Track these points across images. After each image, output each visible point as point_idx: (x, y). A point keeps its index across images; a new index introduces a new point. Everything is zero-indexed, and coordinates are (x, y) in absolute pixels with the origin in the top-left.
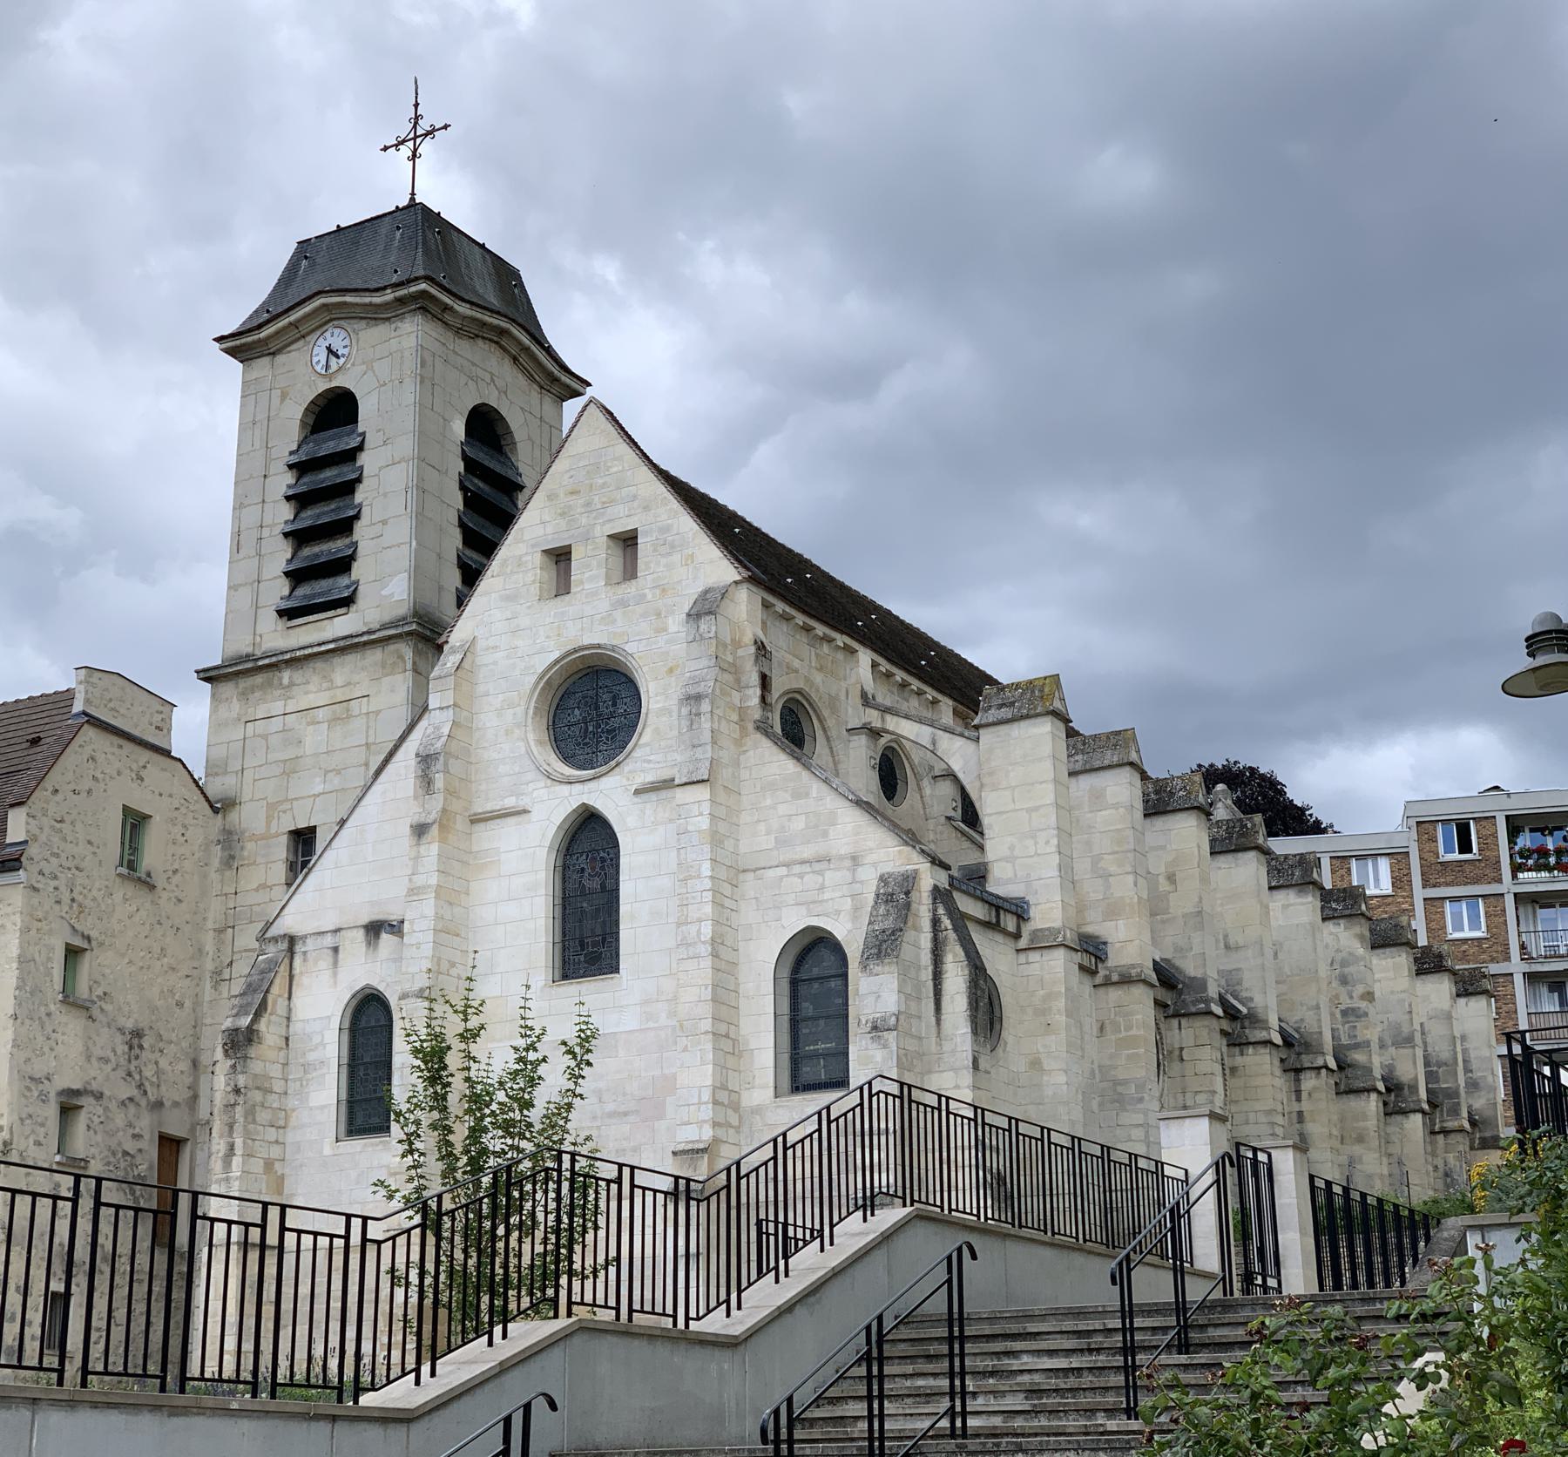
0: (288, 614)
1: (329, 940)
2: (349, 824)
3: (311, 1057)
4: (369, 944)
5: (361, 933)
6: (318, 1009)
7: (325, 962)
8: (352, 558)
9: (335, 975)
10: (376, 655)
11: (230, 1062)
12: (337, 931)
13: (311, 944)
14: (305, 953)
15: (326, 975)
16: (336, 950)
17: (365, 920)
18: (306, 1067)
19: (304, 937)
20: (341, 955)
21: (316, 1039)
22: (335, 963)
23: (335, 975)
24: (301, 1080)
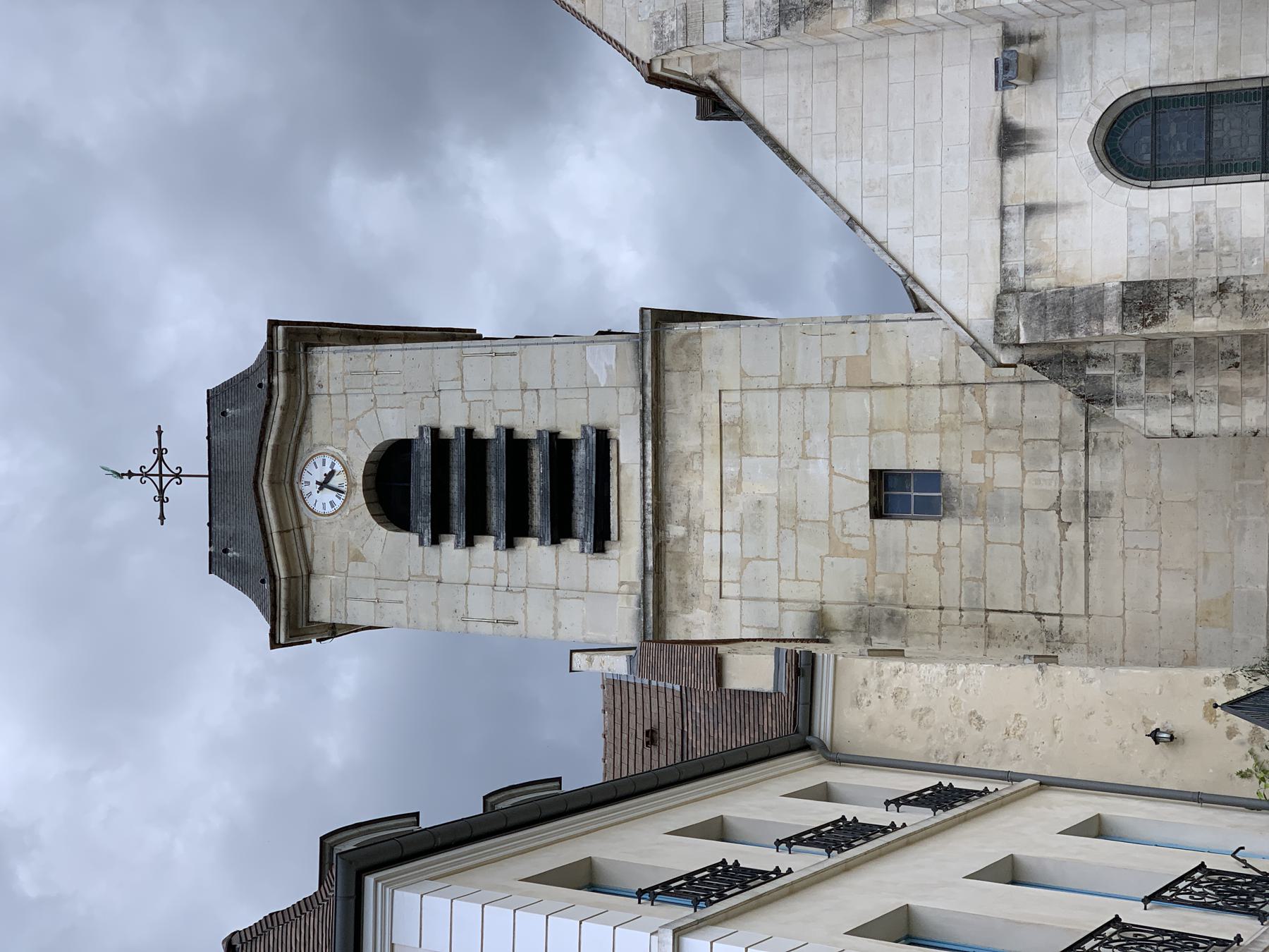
0: (601, 539)
1: (1014, 226)
2: (857, 214)
3: (1186, 239)
4: (1030, 148)
5: (1015, 166)
6: (1112, 232)
7: (1045, 227)
8: (554, 435)
9: (1067, 207)
10: (673, 380)
11: (1175, 311)
12: (1003, 214)
13: (1016, 261)
14: (1027, 270)
15: (1066, 223)
16: (1030, 210)
17: (994, 161)
18: (1202, 248)
19: (1005, 274)
20: (1040, 199)
21: (1161, 233)
22: (1051, 208)
23: (1067, 207)
24: (1220, 256)
